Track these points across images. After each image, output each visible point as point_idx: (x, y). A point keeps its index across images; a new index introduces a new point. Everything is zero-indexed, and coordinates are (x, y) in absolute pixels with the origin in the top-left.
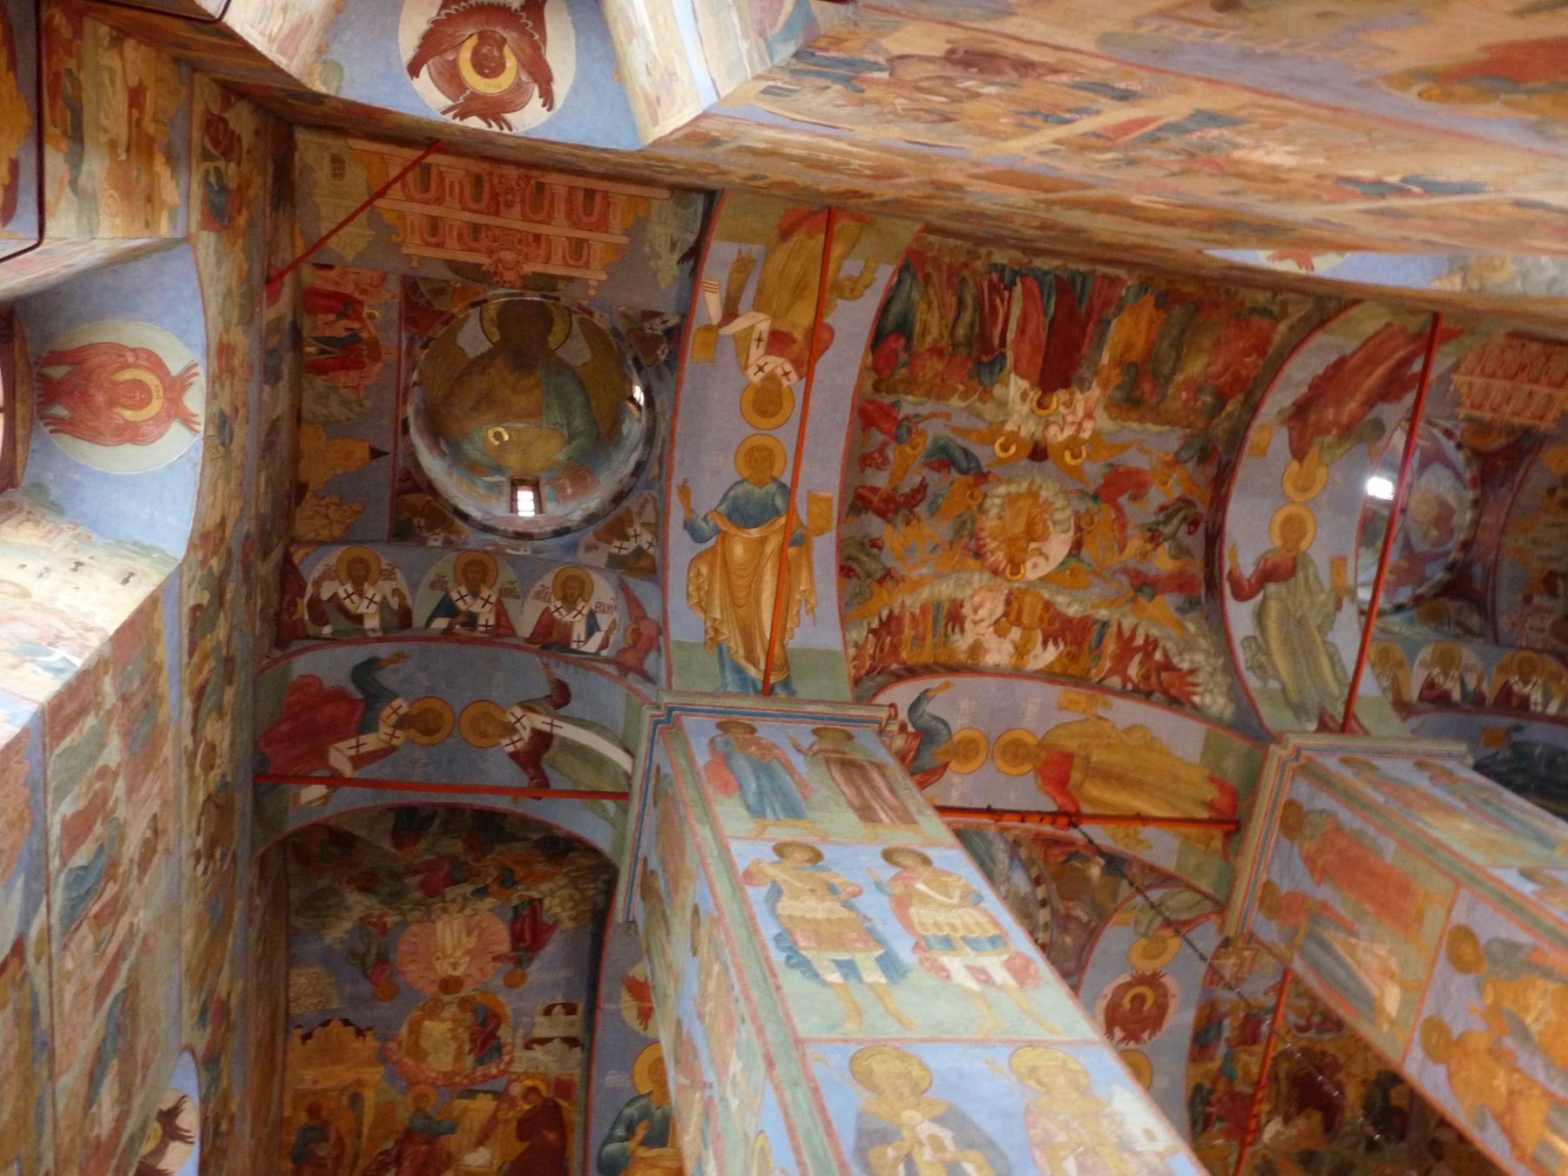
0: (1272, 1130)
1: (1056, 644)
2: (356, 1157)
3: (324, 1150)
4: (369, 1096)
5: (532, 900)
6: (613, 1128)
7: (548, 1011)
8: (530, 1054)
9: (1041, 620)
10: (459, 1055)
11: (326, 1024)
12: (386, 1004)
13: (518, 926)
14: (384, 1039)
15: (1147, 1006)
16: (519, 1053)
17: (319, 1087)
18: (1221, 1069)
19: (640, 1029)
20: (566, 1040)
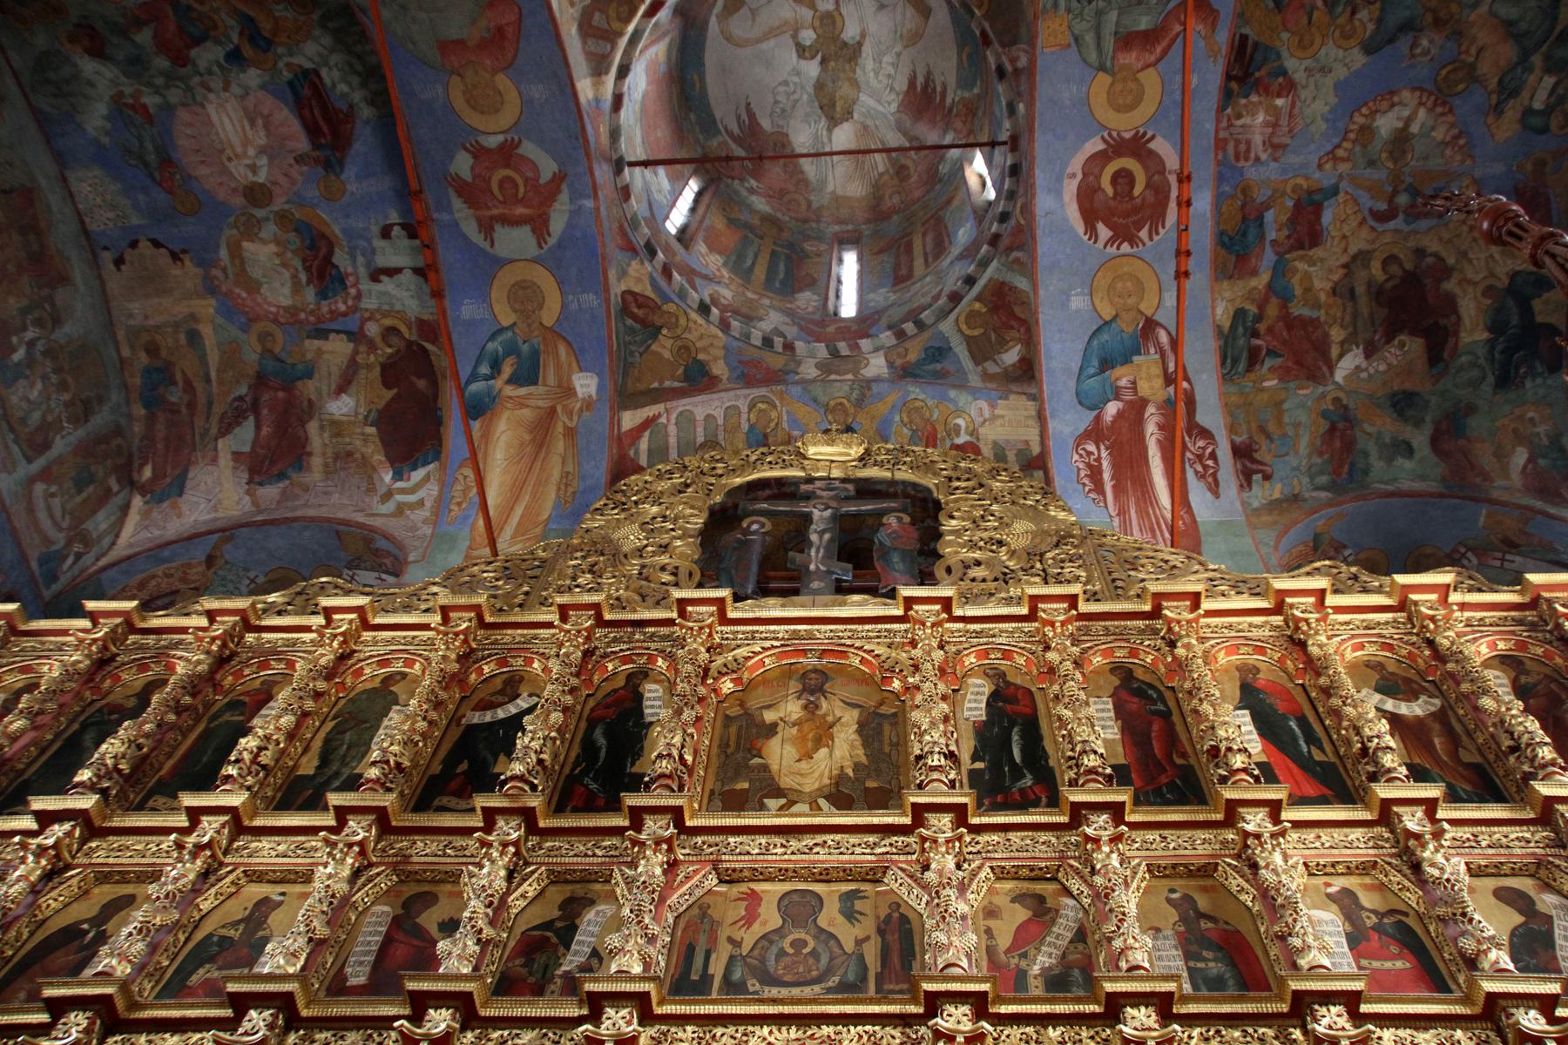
0: (1347, 365)
6: (475, 367)
11: (134, 244)
15: (1138, 190)
16: (366, 285)
18: (1270, 287)
19: (486, 245)
20: (417, 271)
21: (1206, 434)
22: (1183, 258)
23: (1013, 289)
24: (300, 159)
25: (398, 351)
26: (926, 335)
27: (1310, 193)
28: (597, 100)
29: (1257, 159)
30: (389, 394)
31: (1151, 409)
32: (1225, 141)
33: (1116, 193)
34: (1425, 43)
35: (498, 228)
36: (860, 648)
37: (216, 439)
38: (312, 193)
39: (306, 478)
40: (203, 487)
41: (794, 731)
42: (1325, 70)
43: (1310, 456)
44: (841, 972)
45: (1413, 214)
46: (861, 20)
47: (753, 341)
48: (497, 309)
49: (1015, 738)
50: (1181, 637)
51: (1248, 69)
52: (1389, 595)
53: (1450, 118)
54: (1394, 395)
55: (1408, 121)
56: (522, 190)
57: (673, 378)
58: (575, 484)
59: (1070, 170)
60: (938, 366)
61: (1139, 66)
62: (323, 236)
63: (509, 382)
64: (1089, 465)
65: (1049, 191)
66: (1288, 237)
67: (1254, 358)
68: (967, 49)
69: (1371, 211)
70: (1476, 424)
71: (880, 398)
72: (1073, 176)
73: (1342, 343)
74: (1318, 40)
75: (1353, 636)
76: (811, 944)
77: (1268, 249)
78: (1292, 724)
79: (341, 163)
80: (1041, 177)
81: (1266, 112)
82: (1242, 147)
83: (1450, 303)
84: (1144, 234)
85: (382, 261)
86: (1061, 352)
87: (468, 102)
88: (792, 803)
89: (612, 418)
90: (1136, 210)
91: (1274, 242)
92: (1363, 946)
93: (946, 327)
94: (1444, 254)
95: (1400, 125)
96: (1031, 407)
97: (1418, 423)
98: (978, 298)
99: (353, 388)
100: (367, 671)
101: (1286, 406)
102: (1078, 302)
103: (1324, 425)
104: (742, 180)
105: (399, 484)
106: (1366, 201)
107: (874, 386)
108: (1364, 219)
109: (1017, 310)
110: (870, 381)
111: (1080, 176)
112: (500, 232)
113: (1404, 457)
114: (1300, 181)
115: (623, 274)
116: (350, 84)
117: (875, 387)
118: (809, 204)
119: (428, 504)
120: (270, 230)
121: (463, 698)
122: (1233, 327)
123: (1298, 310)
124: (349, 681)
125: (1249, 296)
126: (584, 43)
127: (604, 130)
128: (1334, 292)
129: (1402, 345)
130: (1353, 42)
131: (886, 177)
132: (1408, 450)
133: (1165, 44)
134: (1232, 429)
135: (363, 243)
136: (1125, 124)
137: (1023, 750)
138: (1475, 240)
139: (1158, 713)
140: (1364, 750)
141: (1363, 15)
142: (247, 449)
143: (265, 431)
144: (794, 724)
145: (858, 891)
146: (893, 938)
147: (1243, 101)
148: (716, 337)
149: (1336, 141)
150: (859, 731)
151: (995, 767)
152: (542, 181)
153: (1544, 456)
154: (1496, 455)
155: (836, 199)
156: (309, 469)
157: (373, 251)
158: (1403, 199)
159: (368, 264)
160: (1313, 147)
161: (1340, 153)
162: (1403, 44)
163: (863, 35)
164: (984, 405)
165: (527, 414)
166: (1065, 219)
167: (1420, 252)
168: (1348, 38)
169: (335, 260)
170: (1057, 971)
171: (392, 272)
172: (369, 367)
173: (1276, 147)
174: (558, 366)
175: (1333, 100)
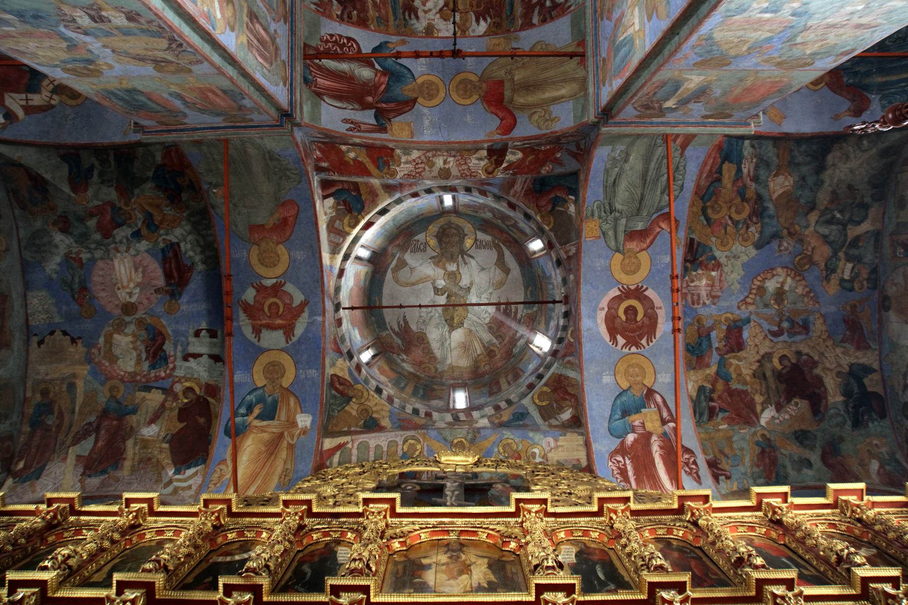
0: (767, 415)
1: (485, 20)
2: (71, 426)
3: (51, 421)
4: (80, 385)
5: (172, 244)
7: (197, 334)
8: (187, 364)
9: (471, 5)
10: (139, 361)
12: (89, 321)
13: (167, 265)
14: (90, 345)
15: (639, 318)
17: (49, 377)
19: (255, 341)
20: (211, 356)
21: (687, 450)
22: (677, 321)
23: (567, 378)
24: (157, 291)
25: (191, 402)
26: (513, 407)
27: (735, 321)
28: (331, 267)
29: (704, 304)
30: (181, 426)
31: (654, 438)
32: (686, 294)
33: (627, 319)
34: (785, 244)
35: (264, 331)
36: (487, 528)
37: (69, 447)
38: (160, 309)
39: (119, 474)
40: (53, 475)
41: (444, 567)
42: (736, 257)
43: (752, 466)
45: (792, 334)
46: (471, 276)
47: (407, 411)
48: (256, 377)
51: (696, 256)
53: (803, 283)
54: (796, 432)
55: (783, 284)
56: (281, 310)
57: (357, 426)
58: (291, 475)
59: (601, 306)
60: (521, 423)
61: (638, 250)
62: (161, 333)
63: (257, 418)
64: (619, 468)
65: (589, 317)
66: (725, 346)
67: (712, 413)
68: (530, 288)
69: (769, 331)
70: (845, 447)
71: (486, 438)
72: (603, 309)
73: (762, 404)
74: (731, 242)
77: (715, 353)
79: (180, 294)
80: (584, 309)
81: (707, 279)
82: (695, 298)
83: (819, 381)
84: (644, 342)
85: (192, 349)
86: (598, 405)
87: (259, 260)
89: (318, 441)
90: (640, 328)
91: (717, 349)
93: (526, 402)
94: (811, 354)
95: (779, 286)
96: (580, 440)
97: (812, 448)
98: (545, 385)
99: (160, 421)
100: (148, 536)
101: (734, 439)
102: (607, 379)
103: (758, 450)
104: (398, 355)
105: (178, 477)
106: (766, 326)
107: (482, 431)
108: (766, 335)
109: (569, 390)
110: (478, 430)
111: (606, 309)
112: (266, 334)
113: (807, 468)
114: (729, 315)
115: (333, 365)
116: (195, 252)
117: (483, 432)
118: (436, 370)
119: (194, 488)
120: (131, 328)
121: (211, 551)
122: (698, 395)
123: (735, 386)
124: (135, 539)
125: (706, 379)
126: (329, 235)
127: (332, 284)
128: (754, 375)
129: (796, 404)
130: (749, 243)
131: (482, 357)
132: (809, 465)
133: (651, 238)
134: (705, 452)
135: (183, 339)
136: (632, 281)
138: (827, 346)
141: (752, 229)
142: (86, 454)
143: (100, 444)
144: (443, 564)
147: (694, 273)
148: (384, 405)
149: (746, 294)
152: (294, 305)
153: (889, 465)
154: (860, 465)
155: (452, 368)
156: (122, 468)
157: (188, 344)
158: (785, 325)
159: (183, 351)
160: (733, 297)
161: (749, 300)
162: (775, 244)
163: (472, 284)
164: (551, 440)
165: (266, 436)
166: (599, 333)
167: (799, 353)
168: (746, 241)
169: (165, 347)
171: (196, 356)
172: (171, 409)
173: (714, 297)
174: (288, 410)
175: (742, 273)
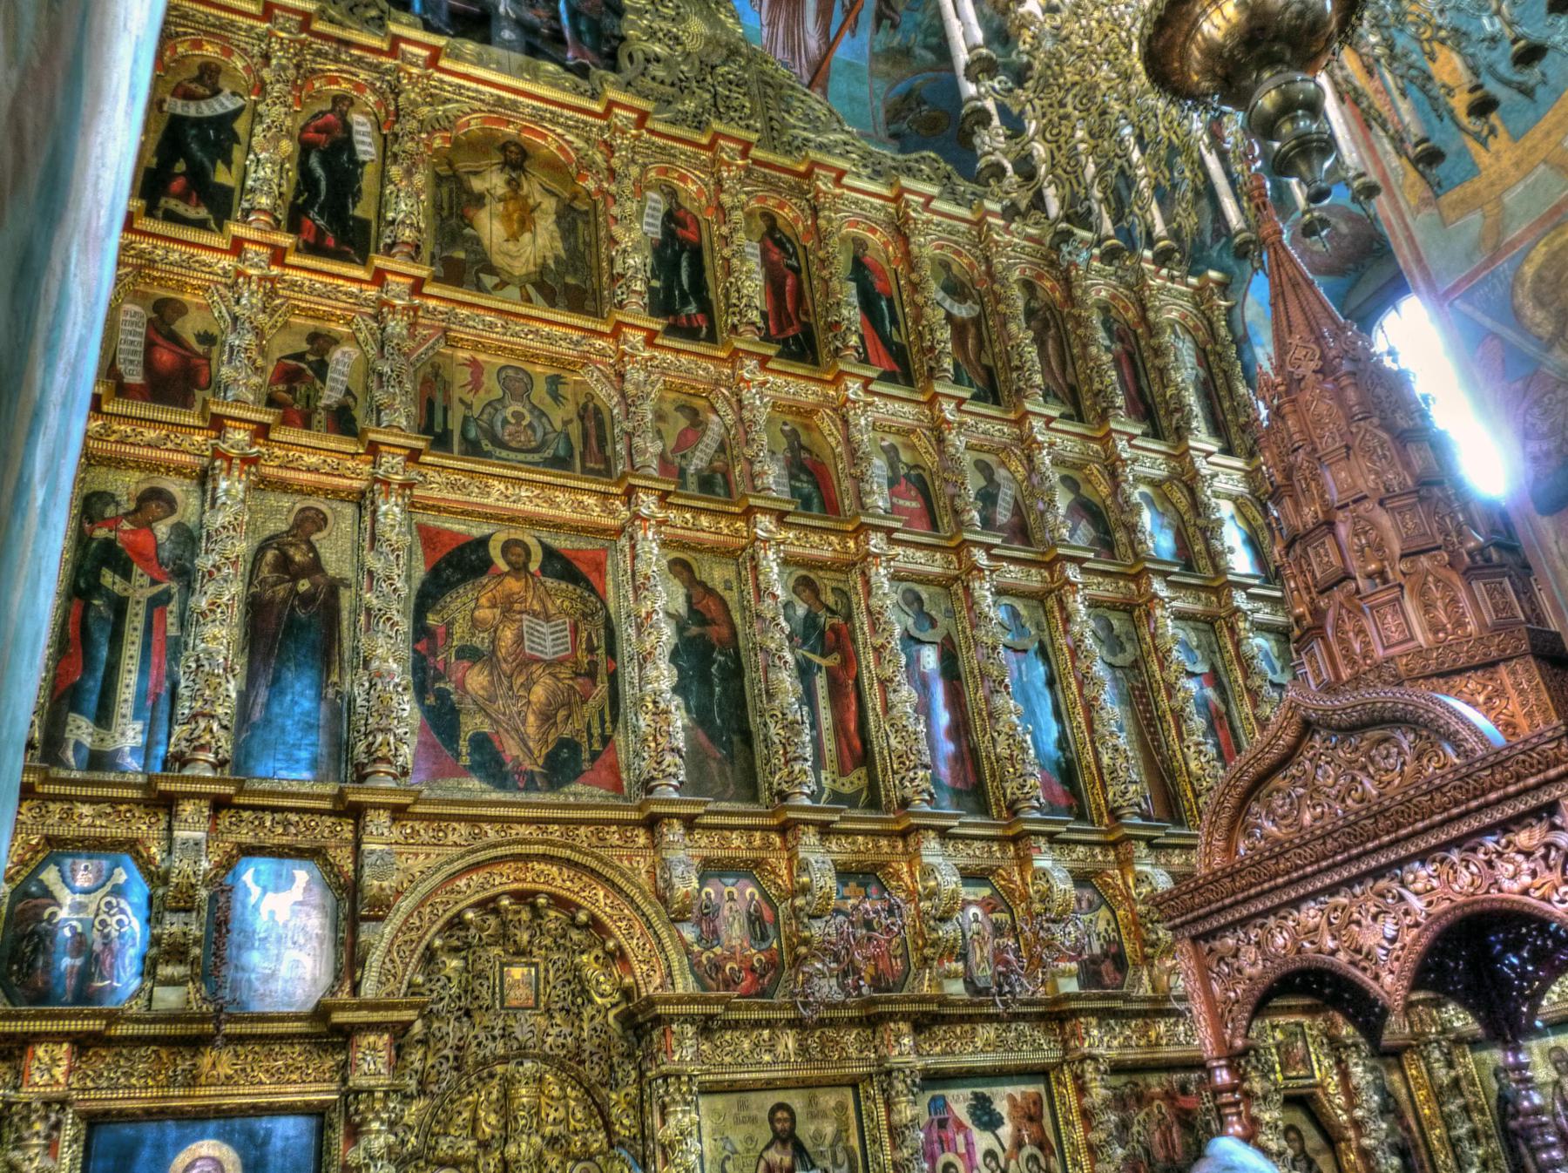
44: (554, 446)
49: (684, 264)
50: (824, 209)
52: (973, 212)
75: (940, 238)
76: (528, 418)
78: (884, 304)
88: (503, 284)
92: (896, 488)
137: (690, 277)
139: (791, 267)
140: (932, 349)
145: (558, 376)
146: (591, 424)
150: (558, 222)
151: (668, 289)
170: (706, 473)
